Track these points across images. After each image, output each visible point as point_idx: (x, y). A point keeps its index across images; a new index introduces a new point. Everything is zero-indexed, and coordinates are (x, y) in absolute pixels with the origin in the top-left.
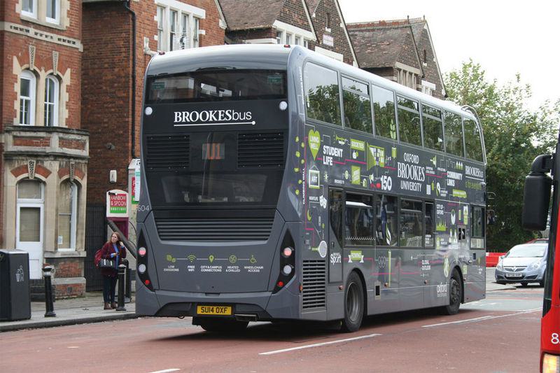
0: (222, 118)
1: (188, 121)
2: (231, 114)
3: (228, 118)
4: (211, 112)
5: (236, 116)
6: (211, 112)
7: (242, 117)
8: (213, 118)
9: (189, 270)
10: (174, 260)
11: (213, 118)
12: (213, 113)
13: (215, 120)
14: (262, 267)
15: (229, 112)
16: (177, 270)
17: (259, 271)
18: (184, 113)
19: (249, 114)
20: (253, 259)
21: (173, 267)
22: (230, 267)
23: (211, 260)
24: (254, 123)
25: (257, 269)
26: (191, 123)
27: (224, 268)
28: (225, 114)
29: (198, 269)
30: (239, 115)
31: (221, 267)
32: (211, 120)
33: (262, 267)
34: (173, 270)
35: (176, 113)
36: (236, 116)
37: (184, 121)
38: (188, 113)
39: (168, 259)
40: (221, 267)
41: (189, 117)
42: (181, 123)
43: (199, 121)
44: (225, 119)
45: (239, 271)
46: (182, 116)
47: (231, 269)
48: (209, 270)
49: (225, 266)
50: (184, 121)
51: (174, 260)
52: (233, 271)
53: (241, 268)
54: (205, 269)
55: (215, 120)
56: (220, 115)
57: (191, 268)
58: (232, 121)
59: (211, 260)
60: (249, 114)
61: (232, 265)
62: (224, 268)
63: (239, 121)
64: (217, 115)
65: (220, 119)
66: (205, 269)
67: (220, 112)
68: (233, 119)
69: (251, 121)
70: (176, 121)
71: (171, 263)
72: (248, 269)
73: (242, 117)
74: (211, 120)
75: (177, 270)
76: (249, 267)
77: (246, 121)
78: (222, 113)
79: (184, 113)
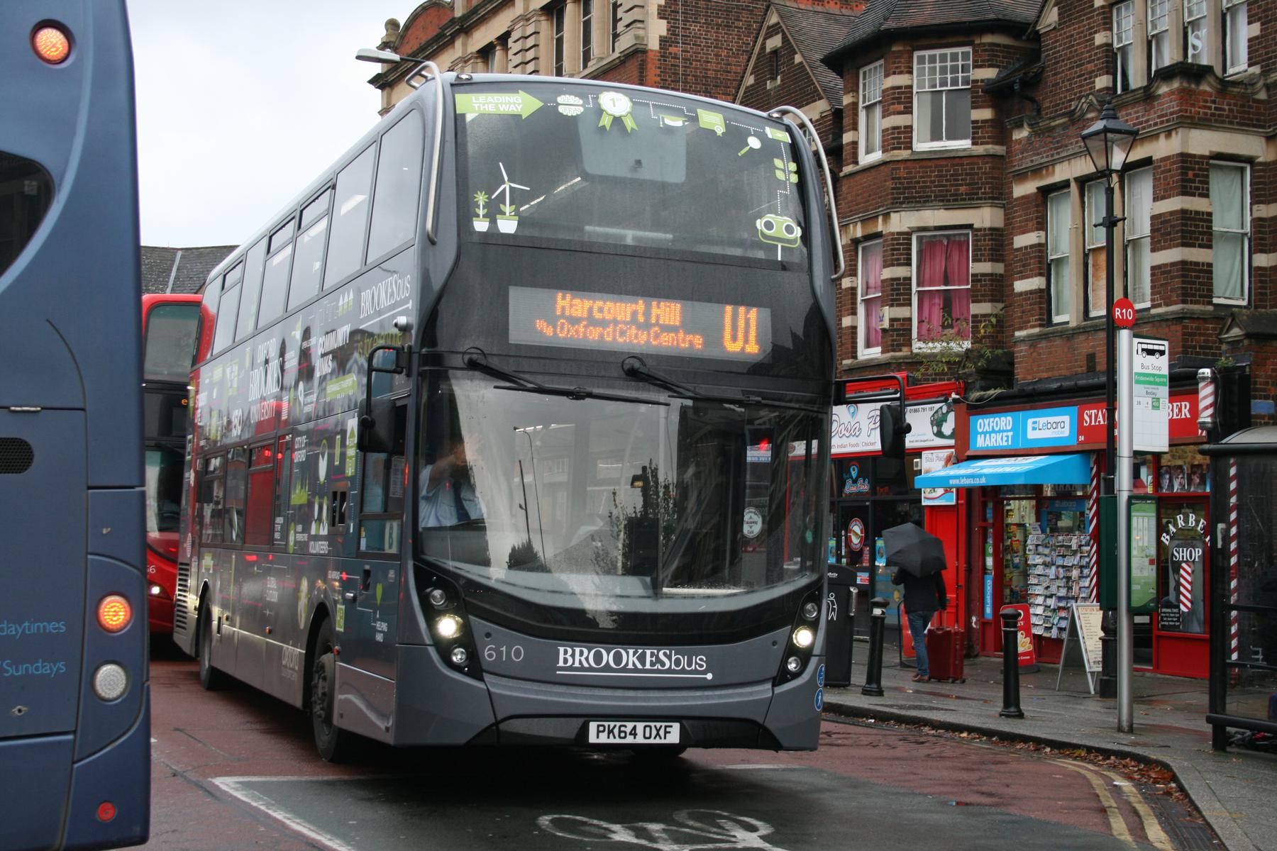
0: (652, 664)
1: (586, 665)
2: (669, 657)
3: (663, 664)
6: (631, 652)
8: (634, 664)
11: (634, 664)
12: (634, 654)
13: (639, 666)
15: (665, 654)
18: (577, 650)
26: (591, 669)
28: (657, 657)
32: (630, 666)
35: (562, 649)
37: (577, 664)
38: (585, 651)
41: (587, 659)
42: (571, 668)
43: (607, 668)
44: (658, 666)
46: (573, 656)
50: (577, 664)
55: (639, 666)
58: (670, 671)
64: (642, 659)
65: (648, 666)
67: (648, 652)
70: (561, 664)
74: (630, 666)
78: (652, 655)
79: (577, 650)
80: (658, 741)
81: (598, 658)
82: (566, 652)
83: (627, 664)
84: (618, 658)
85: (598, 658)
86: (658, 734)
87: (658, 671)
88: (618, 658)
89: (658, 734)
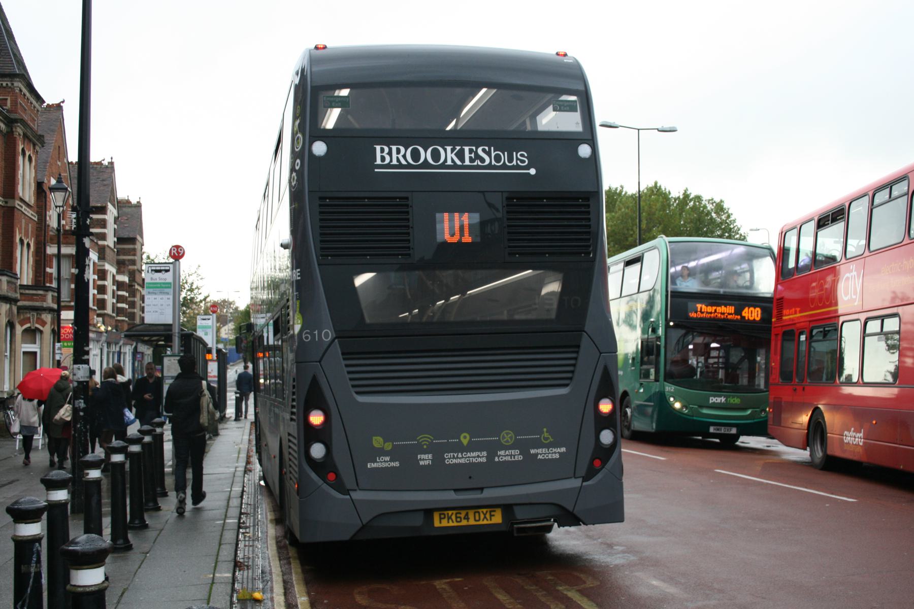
0: (471, 160)
1: (404, 162)
2: (489, 154)
3: (483, 160)
4: (449, 148)
5: (498, 158)
6: (449, 148)
7: (510, 160)
8: (453, 161)
9: (421, 463)
10: (388, 446)
11: (453, 161)
12: (452, 151)
13: (459, 163)
14: (563, 450)
15: (484, 150)
16: (397, 464)
17: (557, 456)
18: (394, 148)
19: (522, 155)
20: (546, 435)
21: (388, 459)
22: (502, 453)
23: (465, 442)
24: (533, 171)
25: (554, 453)
26: (409, 166)
27: (491, 455)
28: (476, 153)
29: (438, 459)
30: (504, 157)
31: (485, 453)
32: (449, 162)
33: (563, 450)
34: (386, 465)
35: (378, 148)
36: (498, 158)
37: (395, 162)
38: (402, 149)
39: (376, 445)
40: (485, 453)
41: (404, 156)
42: (389, 166)
43: (426, 164)
44: (478, 162)
45: (520, 458)
46: (390, 153)
47: (504, 456)
48: (462, 461)
49: (492, 449)
50: (395, 162)
51: (388, 446)
52: (508, 458)
53: (524, 452)
54: (452, 459)
55: (459, 163)
56: (467, 156)
57: (425, 459)
58: (490, 166)
59: (465, 442)
60: (522, 155)
61: (506, 448)
62: (491, 455)
63: (504, 167)
64: (461, 155)
65: (467, 162)
66: (452, 459)
67: (467, 149)
68: (493, 162)
69: (527, 167)
70: (379, 162)
71: (382, 452)
72: (537, 454)
73: (510, 160)
74: (449, 162)
75: (397, 464)
76: (540, 451)
77: (517, 167)
78: (471, 151)
79: (394, 148)
80: (485, 522)
81: (416, 155)
82: (382, 150)
83: (446, 160)
84: (436, 155)
85: (416, 155)
86: (485, 517)
87: (478, 167)
88: (436, 155)
89: (485, 517)
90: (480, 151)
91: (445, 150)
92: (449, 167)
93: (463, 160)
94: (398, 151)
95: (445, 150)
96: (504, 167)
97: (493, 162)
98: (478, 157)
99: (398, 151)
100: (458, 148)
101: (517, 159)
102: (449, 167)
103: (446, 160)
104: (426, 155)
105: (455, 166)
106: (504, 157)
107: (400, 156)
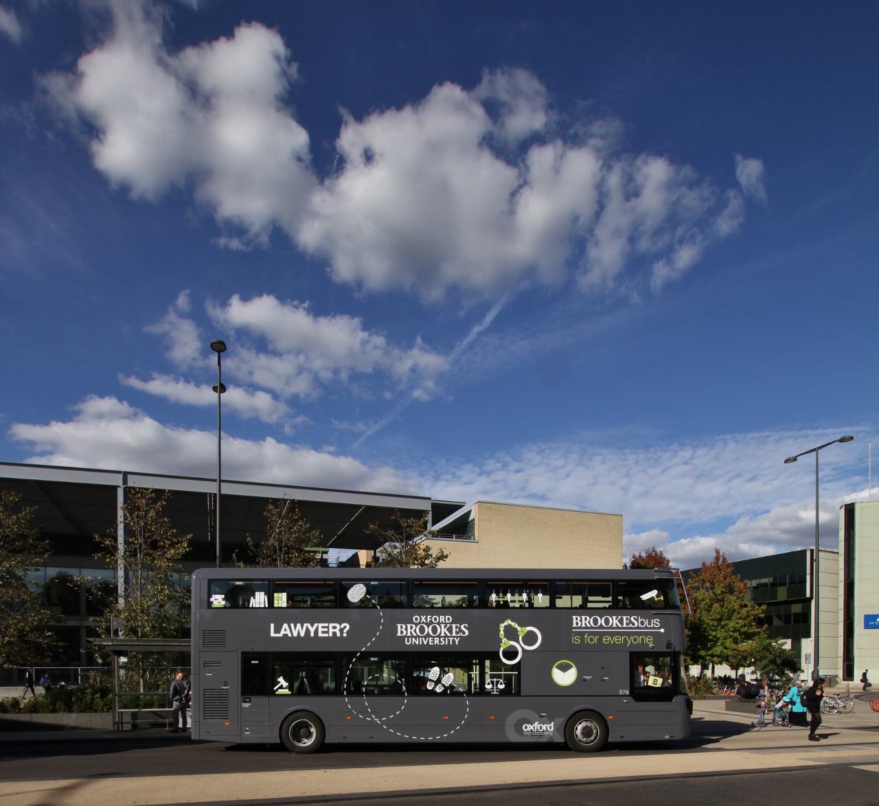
0: (627, 624)
1: (589, 626)
2: (637, 620)
3: (634, 624)
4: (614, 617)
5: (642, 623)
6: (614, 617)
7: (650, 624)
8: (616, 624)
11: (616, 624)
12: (616, 619)
13: (620, 626)
15: (634, 618)
18: (583, 617)
24: (662, 630)
26: (592, 628)
28: (630, 620)
30: (646, 622)
32: (614, 626)
36: (642, 623)
37: (584, 625)
38: (588, 618)
41: (589, 622)
43: (601, 627)
44: (631, 625)
46: (581, 620)
50: (584, 625)
55: (620, 626)
60: (657, 621)
63: (646, 628)
64: (621, 621)
65: (625, 625)
67: (625, 618)
68: (640, 625)
69: (659, 628)
70: (575, 625)
73: (650, 624)
74: (614, 626)
77: (654, 628)
78: (627, 619)
79: (583, 617)
81: (595, 621)
82: (577, 619)
83: (612, 624)
84: (607, 621)
85: (595, 621)
88: (607, 621)
90: (632, 619)
91: (612, 619)
92: (615, 628)
93: (622, 624)
94: (586, 619)
95: (612, 619)
96: (646, 628)
97: (640, 625)
98: (631, 622)
99: (586, 619)
100: (620, 617)
101: (654, 623)
102: (615, 628)
103: (612, 624)
104: (601, 621)
105: (618, 628)
106: (646, 622)
107: (587, 622)
